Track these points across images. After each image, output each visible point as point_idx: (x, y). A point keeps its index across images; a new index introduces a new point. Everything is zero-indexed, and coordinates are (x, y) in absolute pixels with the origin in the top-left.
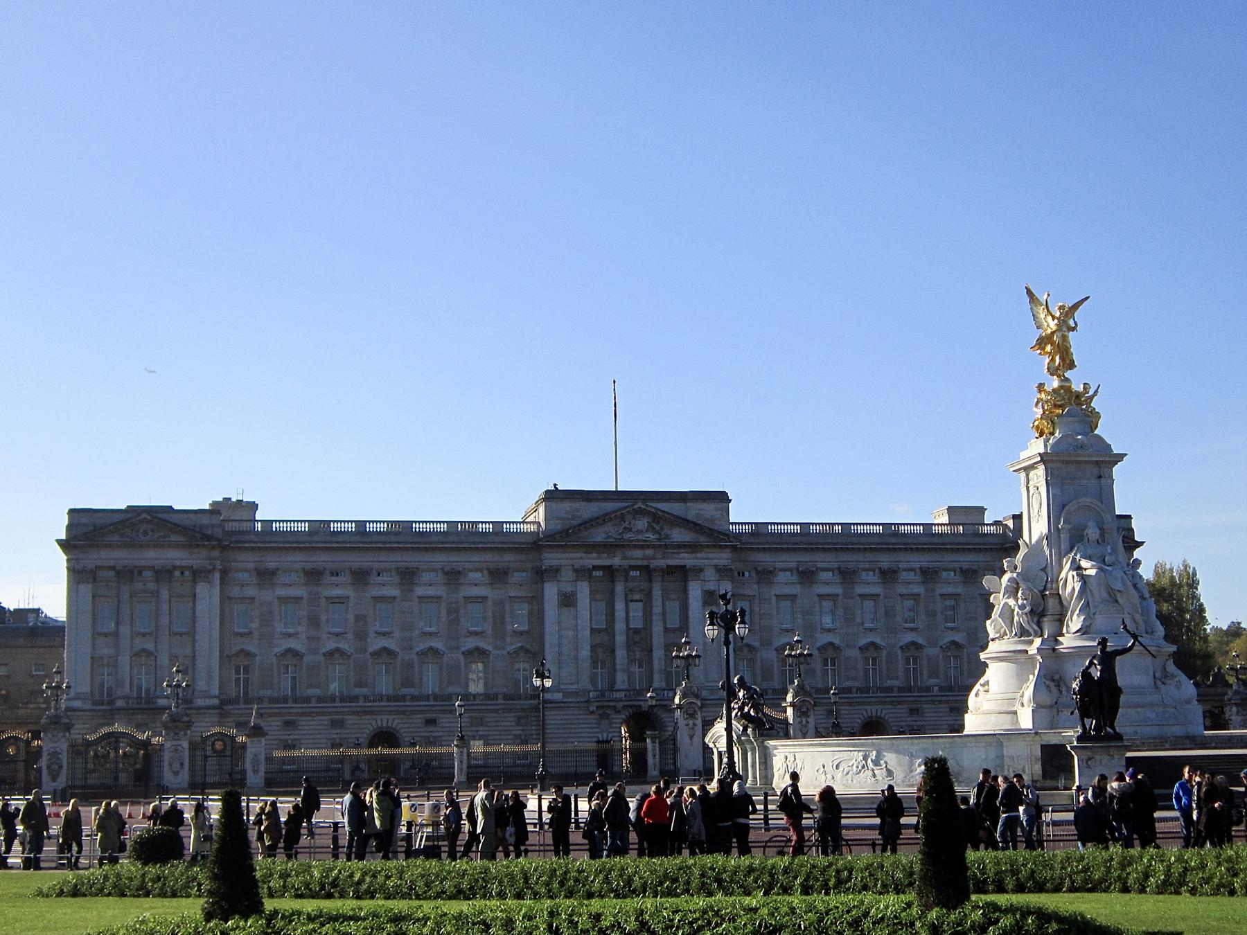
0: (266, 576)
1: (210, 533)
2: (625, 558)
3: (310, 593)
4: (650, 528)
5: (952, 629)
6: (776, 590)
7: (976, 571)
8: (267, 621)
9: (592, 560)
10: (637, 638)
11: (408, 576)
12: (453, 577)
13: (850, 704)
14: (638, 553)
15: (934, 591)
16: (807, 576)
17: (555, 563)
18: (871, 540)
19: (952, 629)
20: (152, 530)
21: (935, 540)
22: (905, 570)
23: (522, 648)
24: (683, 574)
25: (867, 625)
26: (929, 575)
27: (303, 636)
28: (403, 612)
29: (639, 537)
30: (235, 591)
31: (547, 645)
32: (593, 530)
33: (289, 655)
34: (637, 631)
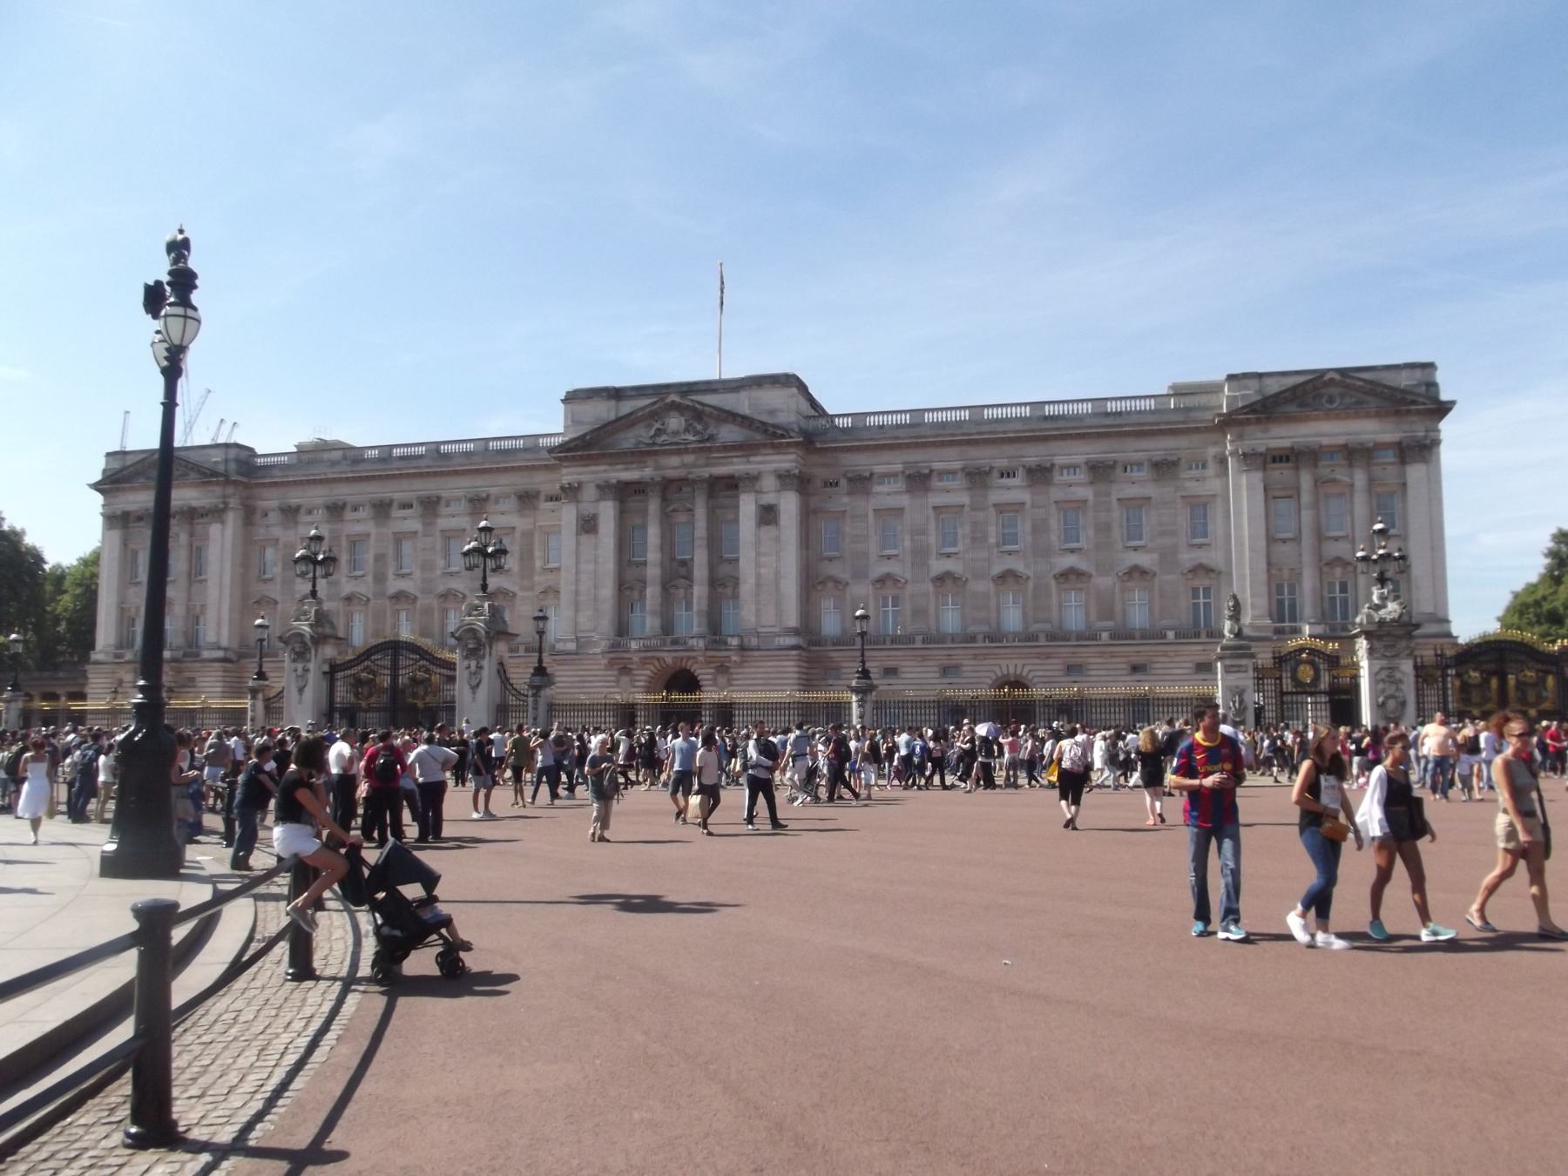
1: (221, 468)
2: (658, 468)
3: (331, 531)
5: (1136, 549)
6: (874, 503)
10: (683, 571)
13: (975, 657)
14: (674, 461)
15: (1108, 494)
16: (918, 481)
18: (1010, 427)
19: (1136, 549)
21: (1109, 421)
22: (1062, 467)
24: (732, 485)
26: (1100, 471)
30: (260, 533)
31: (562, 583)
32: (622, 435)
34: (684, 563)
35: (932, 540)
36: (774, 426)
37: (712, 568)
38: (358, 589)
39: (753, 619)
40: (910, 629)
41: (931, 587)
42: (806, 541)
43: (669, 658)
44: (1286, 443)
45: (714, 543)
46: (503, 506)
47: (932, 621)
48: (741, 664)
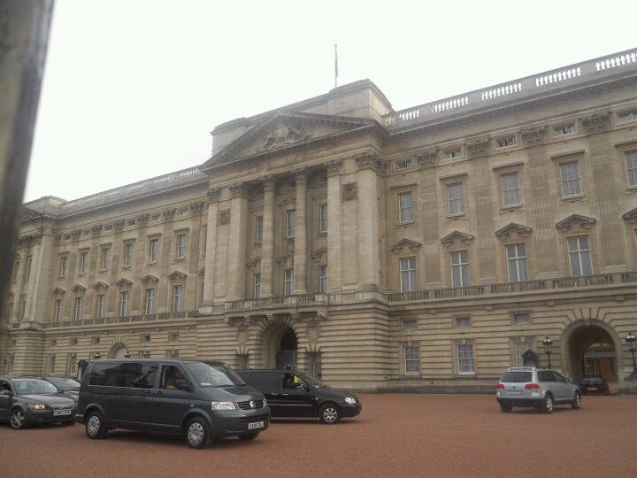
3: (93, 245)
8: (72, 268)
10: (290, 248)
14: (281, 161)
16: (479, 150)
22: (623, 114)
25: (565, 197)
27: (87, 276)
28: (138, 250)
35: (495, 198)
36: (351, 119)
37: (309, 243)
39: (339, 279)
40: (478, 282)
41: (496, 241)
42: (384, 211)
45: (309, 222)
46: (185, 214)
47: (499, 273)
48: (324, 319)
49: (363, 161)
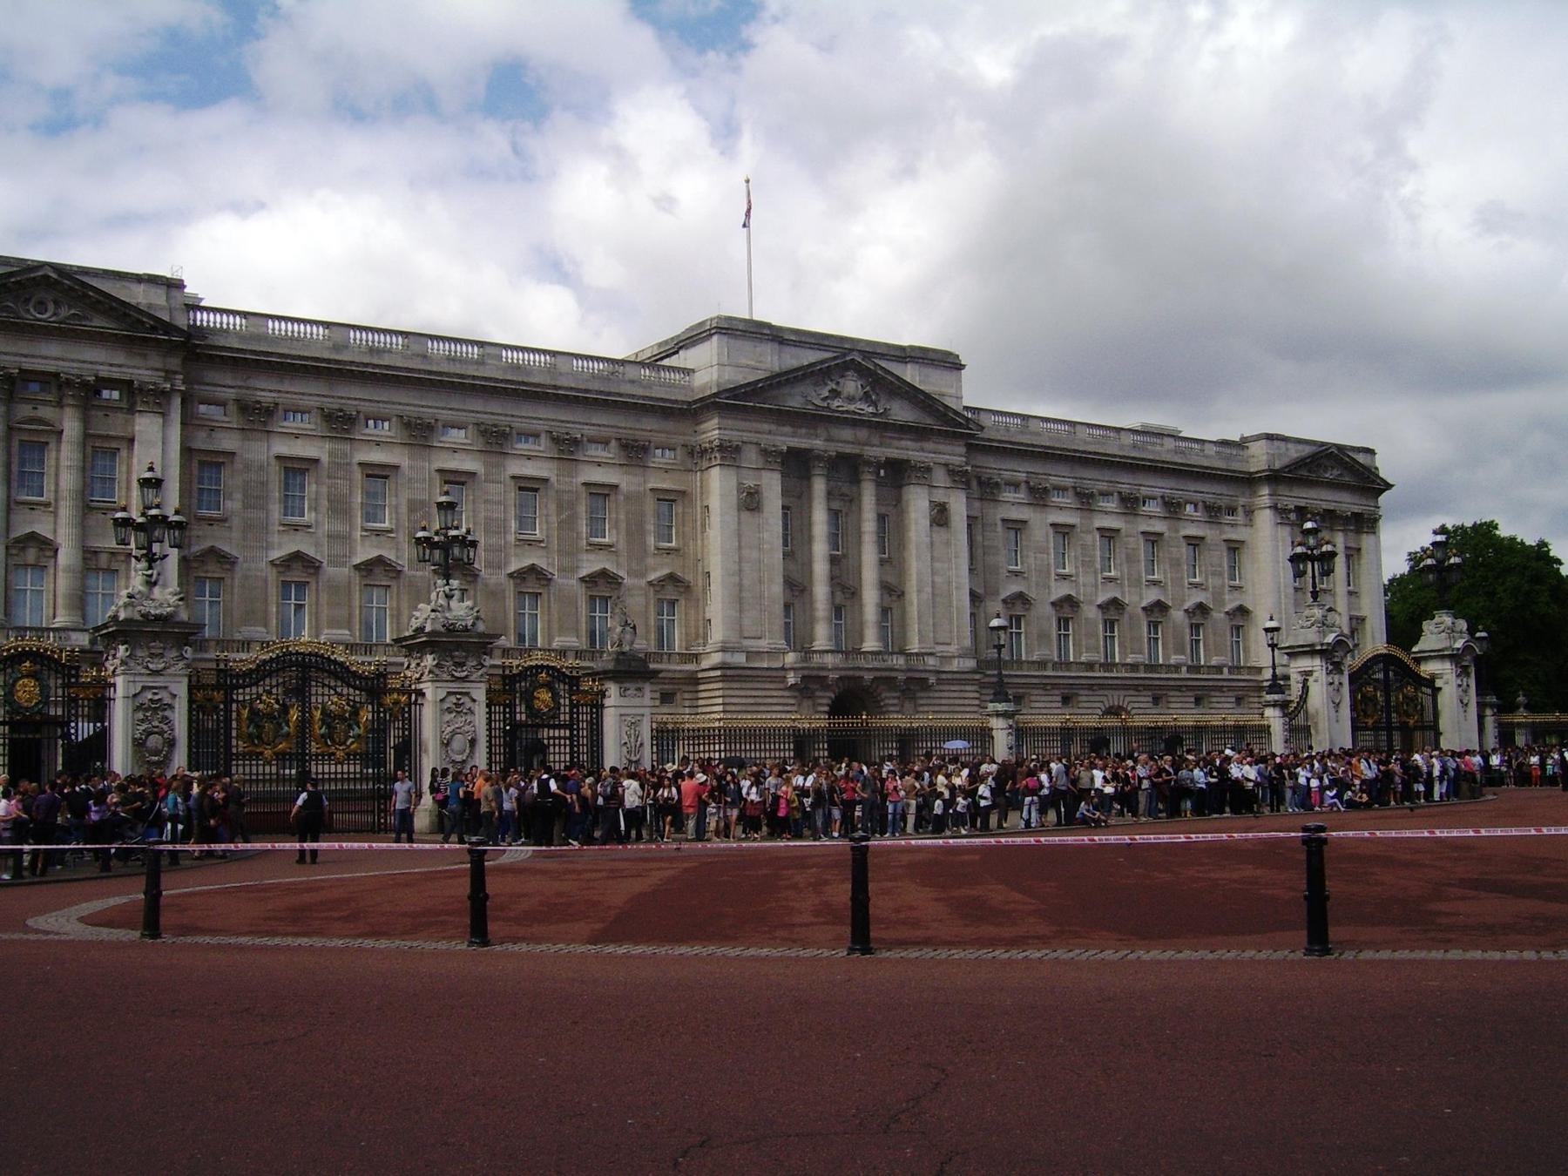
0: (258, 417)
2: (829, 439)
4: (866, 397)
7: (1220, 508)
8: (255, 499)
9: (786, 439)
11: (495, 440)
12: (567, 448)
13: (1091, 687)
14: (847, 433)
15: (1177, 531)
16: (1039, 496)
17: (734, 436)
20: (57, 303)
23: (672, 578)
29: (852, 407)
32: (786, 390)
33: (297, 565)
36: (956, 413)
38: (385, 553)
43: (868, 676)
44: (1302, 503)
49: (953, 472)
